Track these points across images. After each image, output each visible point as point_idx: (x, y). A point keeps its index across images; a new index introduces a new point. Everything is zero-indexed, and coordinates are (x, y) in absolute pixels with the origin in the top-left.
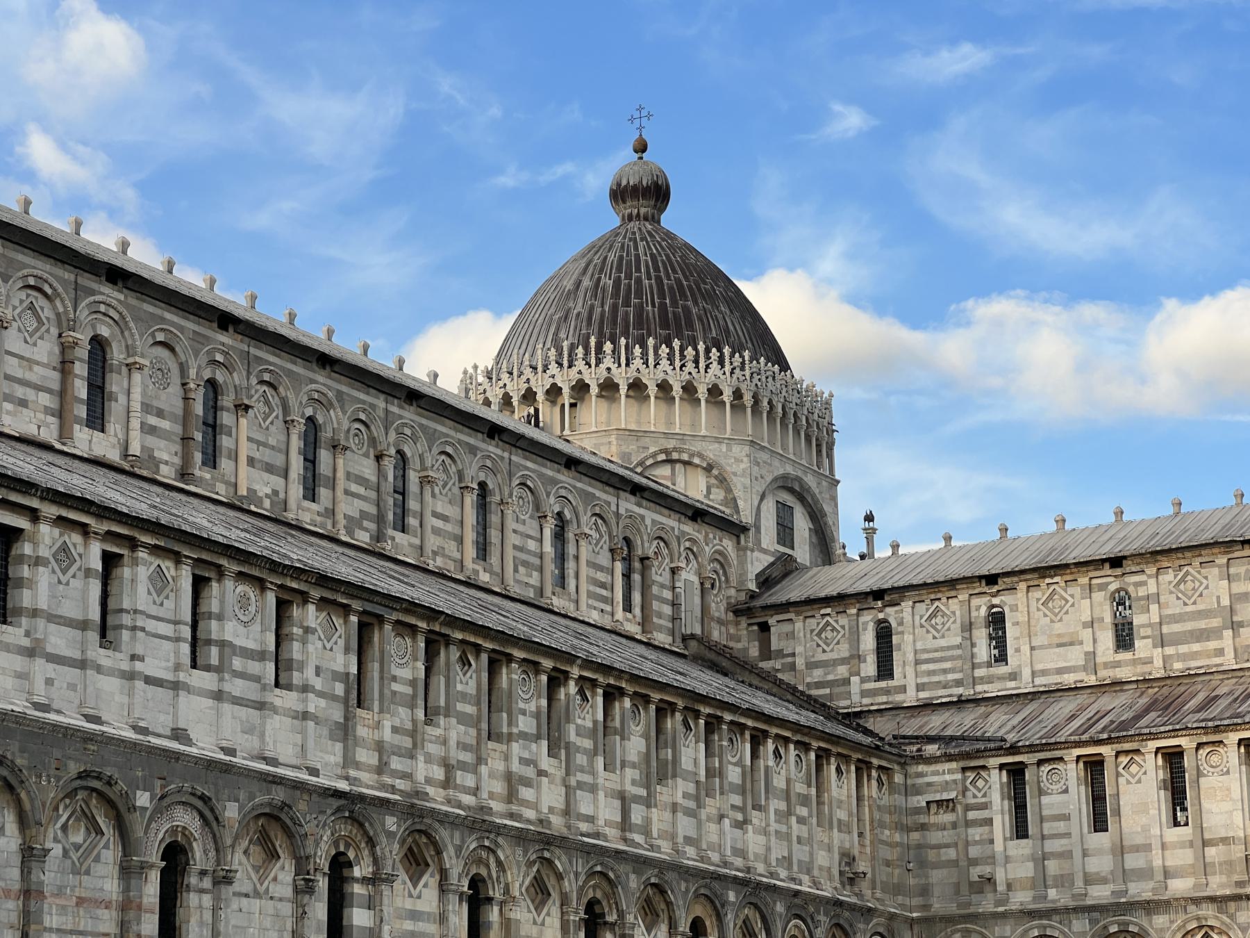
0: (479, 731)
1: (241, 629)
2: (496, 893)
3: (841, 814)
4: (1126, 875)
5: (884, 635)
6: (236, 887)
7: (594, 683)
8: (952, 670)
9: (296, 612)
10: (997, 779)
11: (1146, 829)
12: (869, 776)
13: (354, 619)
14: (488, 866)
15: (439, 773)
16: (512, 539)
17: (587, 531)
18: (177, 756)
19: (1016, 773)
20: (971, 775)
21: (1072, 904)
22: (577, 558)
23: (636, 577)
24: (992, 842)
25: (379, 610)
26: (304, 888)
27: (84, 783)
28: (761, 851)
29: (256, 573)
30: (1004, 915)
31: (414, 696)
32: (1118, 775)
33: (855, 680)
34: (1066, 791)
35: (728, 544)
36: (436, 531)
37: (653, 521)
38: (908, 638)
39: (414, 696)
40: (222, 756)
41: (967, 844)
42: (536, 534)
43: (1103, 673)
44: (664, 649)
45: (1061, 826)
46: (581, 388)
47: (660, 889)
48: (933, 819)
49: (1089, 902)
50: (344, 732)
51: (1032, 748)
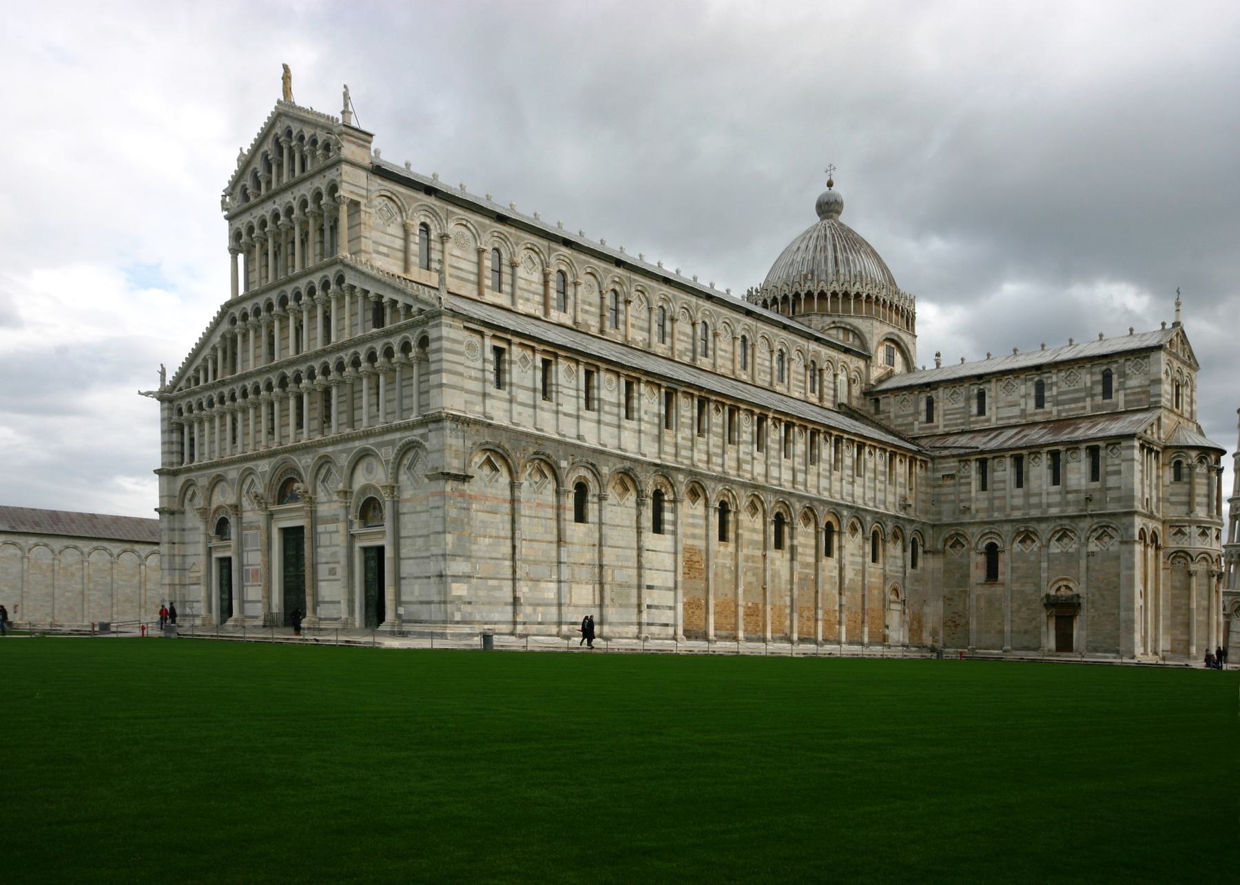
0: (724, 439)
1: (609, 394)
2: (732, 508)
4: (1031, 506)
5: (930, 403)
6: (609, 501)
7: (780, 420)
9: (635, 387)
10: (974, 466)
11: (1040, 486)
12: (916, 464)
13: (663, 390)
14: (728, 497)
15: (704, 457)
16: (758, 360)
17: (793, 357)
18: (579, 447)
19: (983, 464)
20: (963, 464)
21: (1004, 518)
22: (789, 369)
23: (817, 378)
24: (970, 492)
25: (675, 386)
26: (640, 503)
27: (537, 456)
28: (862, 494)
29: (616, 369)
30: (973, 523)
31: (692, 424)
33: (916, 423)
34: (1005, 470)
35: (862, 364)
36: (722, 357)
38: (941, 404)
39: (692, 424)
40: (600, 447)
41: (960, 493)
42: (769, 358)
44: (829, 410)
45: (1002, 485)
46: (797, 295)
47: (810, 509)
48: (945, 482)
49: (1012, 518)
50: (659, 438)
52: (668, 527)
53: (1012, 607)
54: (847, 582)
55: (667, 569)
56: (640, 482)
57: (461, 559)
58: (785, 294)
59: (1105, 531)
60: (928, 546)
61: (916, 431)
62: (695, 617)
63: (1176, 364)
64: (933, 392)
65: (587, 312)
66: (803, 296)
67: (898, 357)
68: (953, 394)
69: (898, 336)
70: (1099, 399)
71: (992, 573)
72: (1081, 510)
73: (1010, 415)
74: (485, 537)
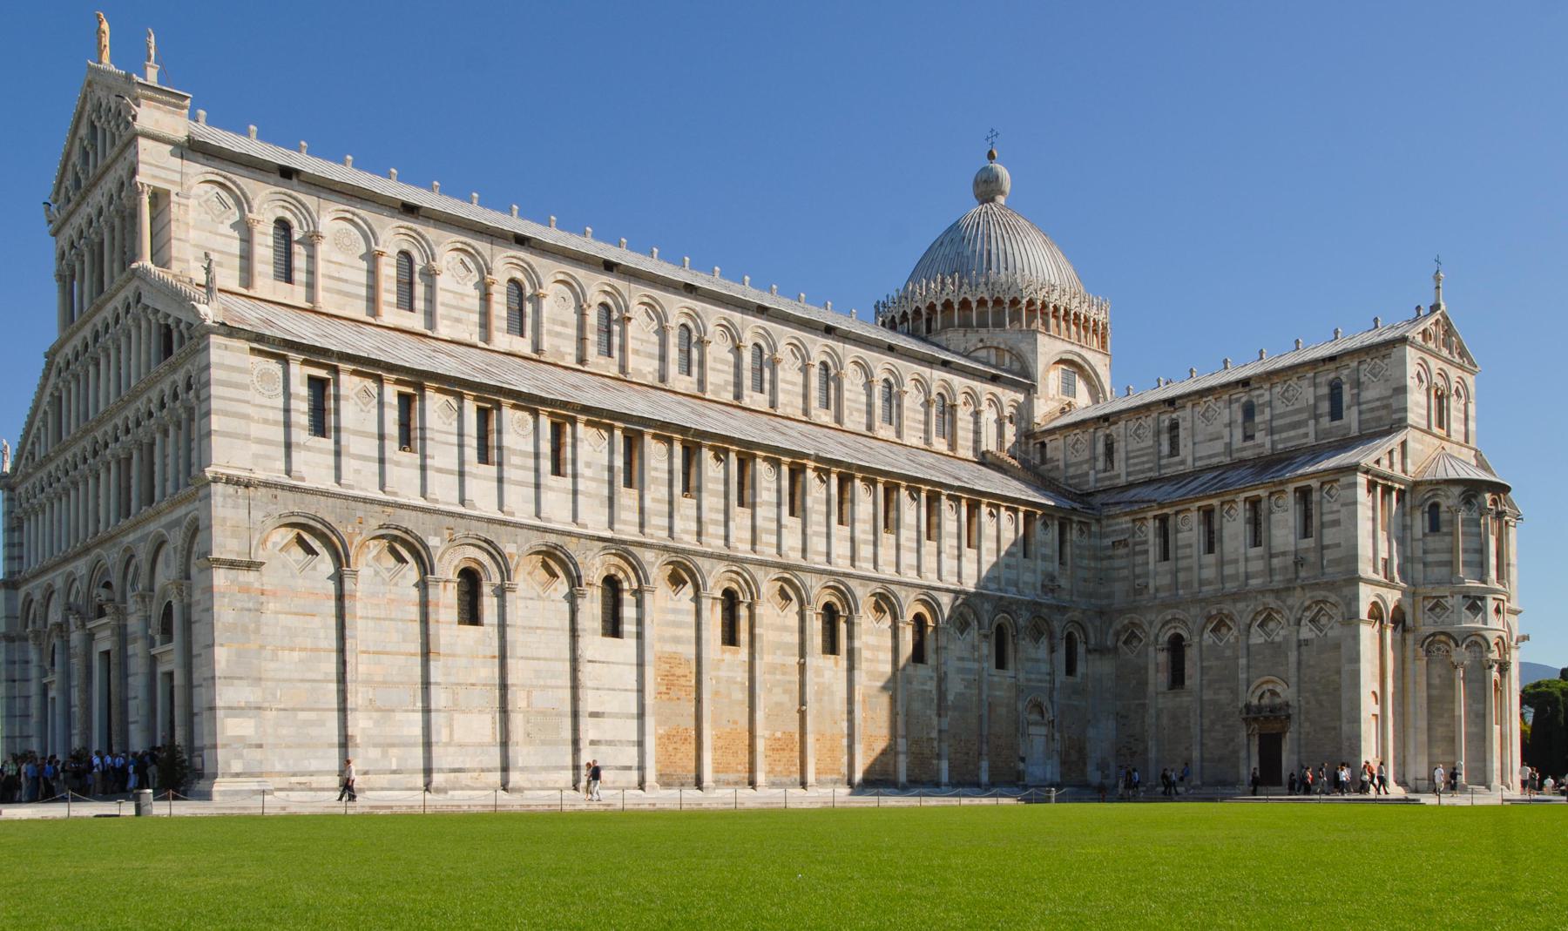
2: (744, 598)
3: (1048, 551)
6: (518, 593)
8: (1147, 462)
10: (1151, 526)
16: (846, 395)
19: (1163, 520)
20: (1138, 524)
24: (1147, 563)
32: (1222, 517)
34: (1191, 530)
35: (1021, 397)
37: (960, 383)
43: (1236, 455)
45: (1188, 550)
46: (932, 307)
51: (1172, 504)
52: (629, 627)
53: (1201, 725)
54: (951, 697)
55: (629, 687)
56: (575, 565)
57: (244, 682)
58: (917, 307)
59: (1321, 609)
60: (1092, 641)
61: (1092, 484)
62: (679, 755)
63: (1435, 364)
64: (1113, 428)
65: (558, 335)
66: (939, 308)
67: (1081, 386)
68: (1138, 428)
69: (1080, 355)
70: (1325, 422)
71: (1177, 678)
72: (1290, 581)
73: (1211, 452)
74: (292, 649)
